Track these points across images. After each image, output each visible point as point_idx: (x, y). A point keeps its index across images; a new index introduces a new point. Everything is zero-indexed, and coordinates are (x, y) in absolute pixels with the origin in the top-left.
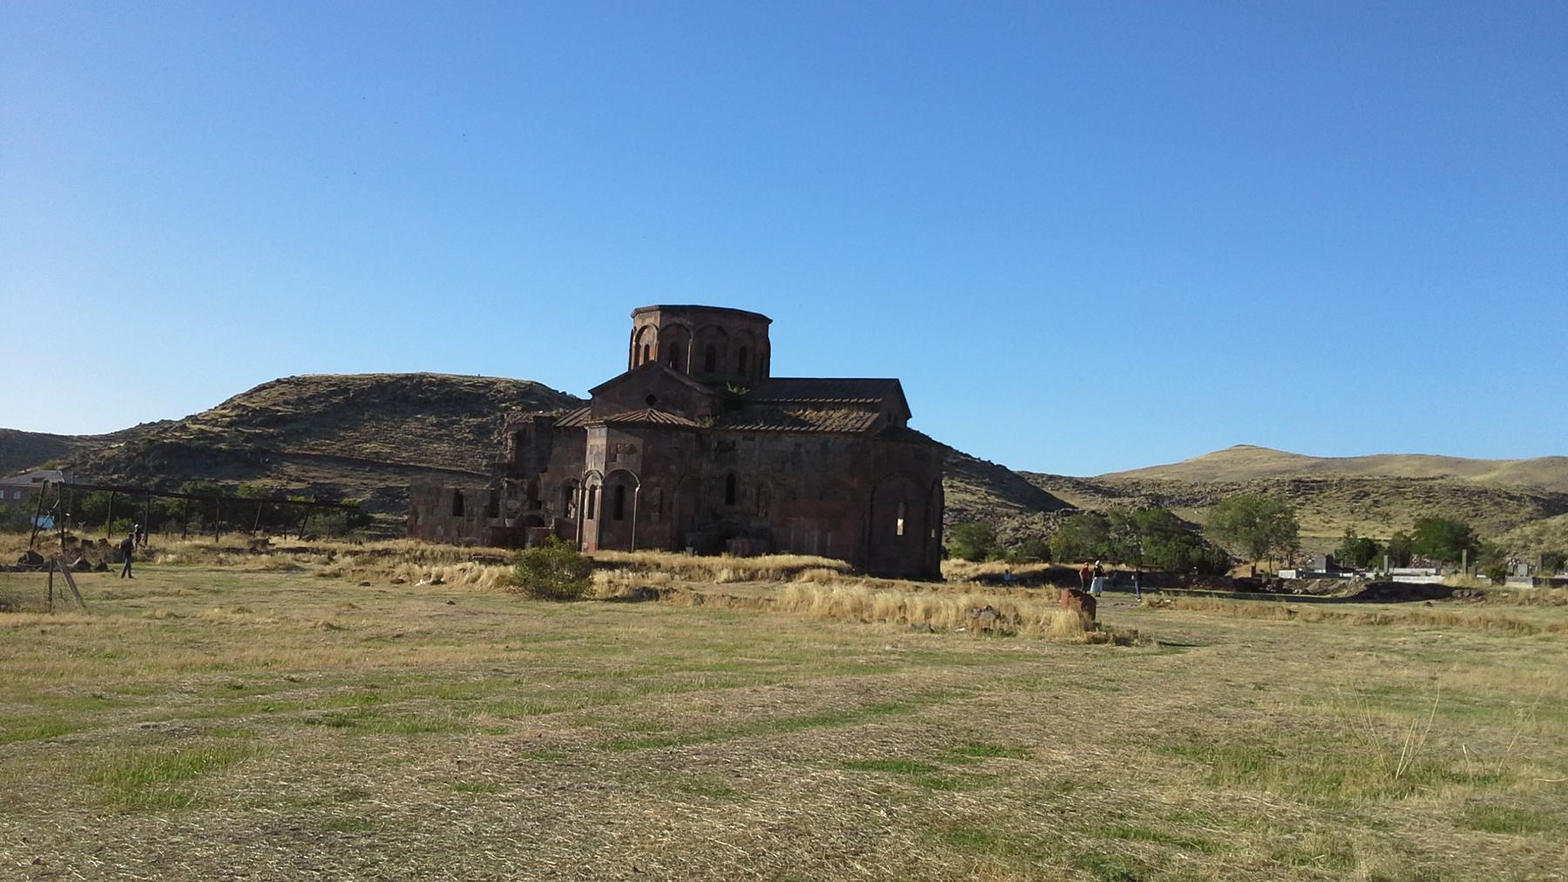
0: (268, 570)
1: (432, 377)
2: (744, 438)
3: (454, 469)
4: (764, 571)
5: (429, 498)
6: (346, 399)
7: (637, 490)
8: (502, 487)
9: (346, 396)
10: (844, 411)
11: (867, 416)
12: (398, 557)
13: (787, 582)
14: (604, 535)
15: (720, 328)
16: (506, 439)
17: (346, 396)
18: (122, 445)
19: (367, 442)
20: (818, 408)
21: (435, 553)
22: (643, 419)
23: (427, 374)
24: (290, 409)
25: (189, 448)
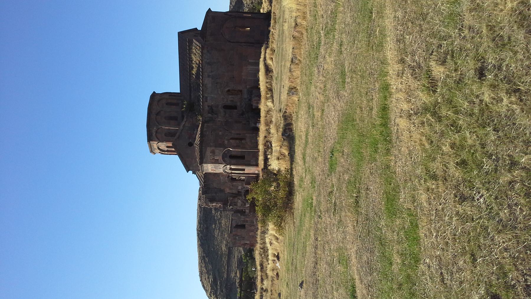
1: (198, 227)
2: (207, 101)
4: (267, 84)
7: (231, 149)
8: (232, 208)
9: (205, 257)
10: (193, 56)
11: (195, 45)
12: (263, 260)
13: (273, 72)
14: (251, 164)
15: (158, 114)
16: (212, 206)
17: (205, 257)
21: (261, 243)
22: (198, 147)
24: (211, 276)
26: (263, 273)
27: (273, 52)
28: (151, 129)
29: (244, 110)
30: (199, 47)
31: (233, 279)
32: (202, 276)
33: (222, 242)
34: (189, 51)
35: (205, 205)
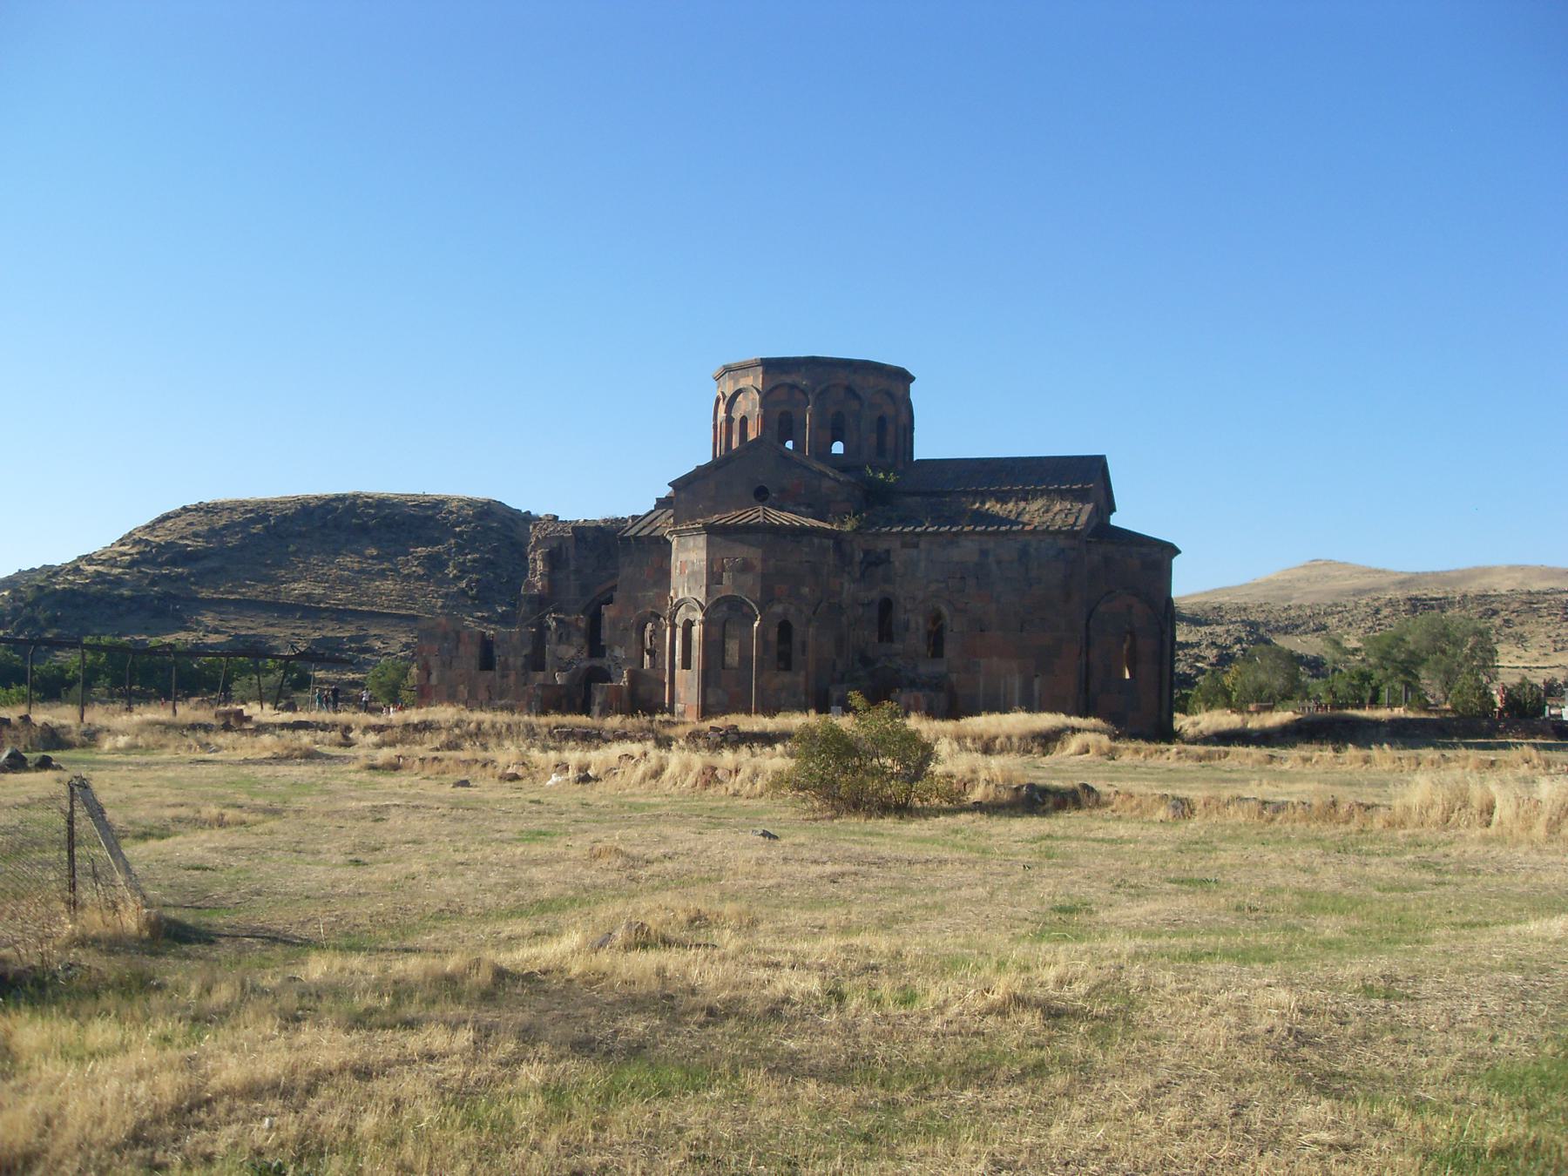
0: (278, 759)
3: (403, 612)
5: (446, 645)
6: (265, 527)
7: (756, 625)
9: (266, 523)
13: (1044, 755)
14: (709, 690)
15: (850, 391)
17: (266, 523)
18: (6, 593)
19: (295, 581)
20: (1003, 499)
21: (498, 725)
23: (361, 493)
24: (201, 543)
25: (85, 595)
26: (398, 730)
27: (1105, 754)
28: (803, 370)
29: (878, 665)
30: (1074, 524)
31: (199, 623)
32: (201, 514)
33: (318, 580)
34: (1054, 491)
35: (537, 538)
